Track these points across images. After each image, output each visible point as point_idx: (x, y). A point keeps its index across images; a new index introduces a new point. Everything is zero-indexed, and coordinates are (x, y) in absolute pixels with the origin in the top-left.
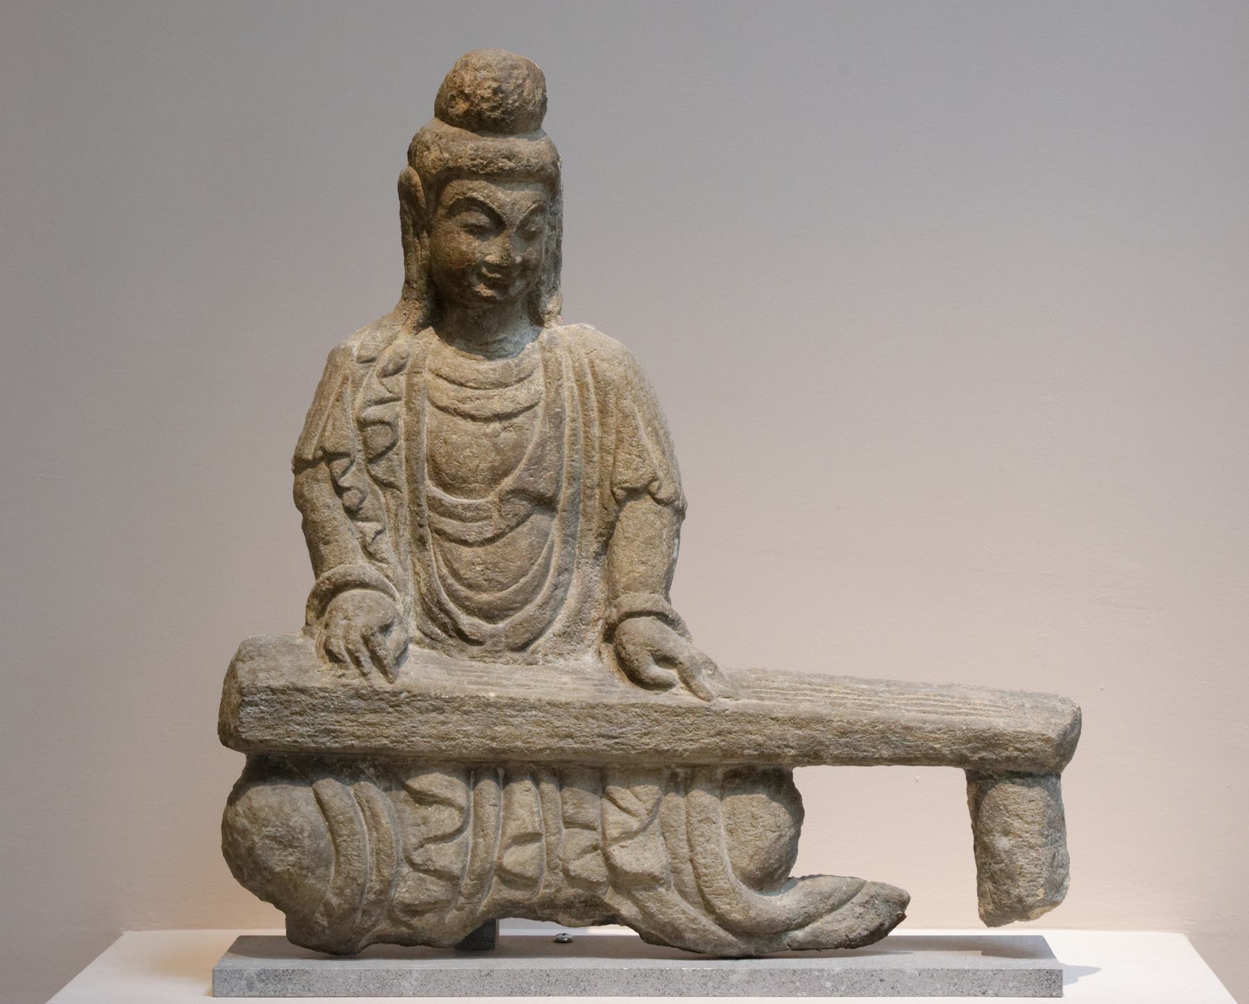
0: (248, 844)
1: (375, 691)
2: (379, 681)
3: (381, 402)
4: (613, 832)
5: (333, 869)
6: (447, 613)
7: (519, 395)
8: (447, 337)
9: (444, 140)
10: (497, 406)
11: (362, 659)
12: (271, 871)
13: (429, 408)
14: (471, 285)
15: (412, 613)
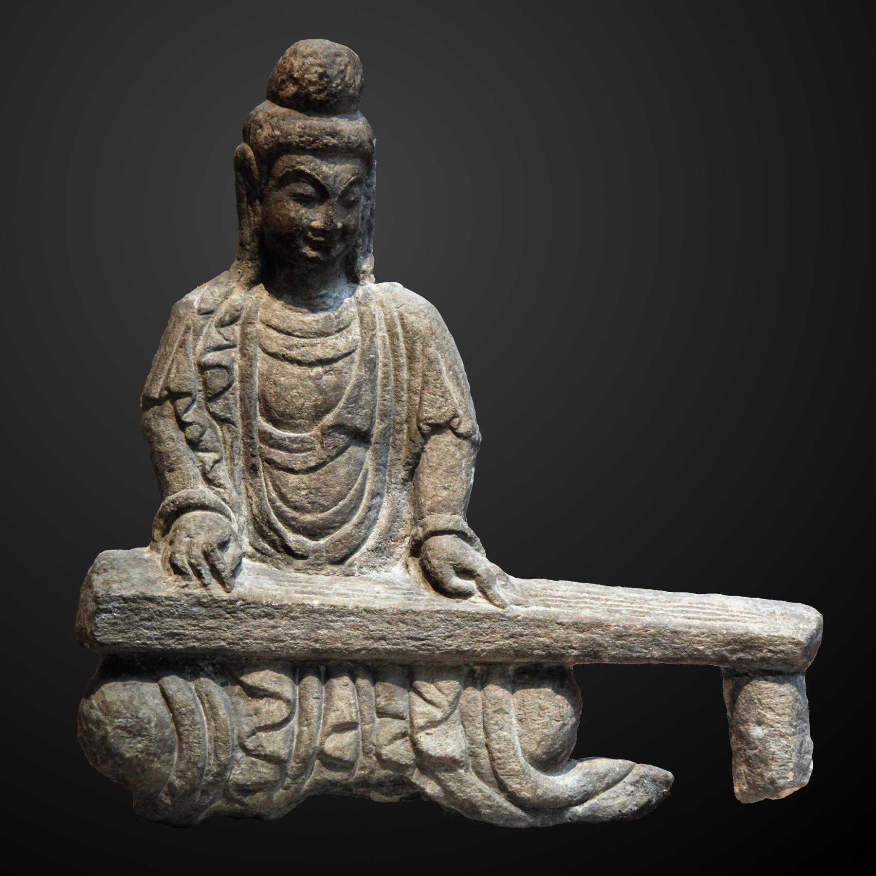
0: (101, 733)
1: (214, 599)
2: (218, 591)
3: (219, 348)
4: (420, 721)
5: (176, 755)
6: (276, 531)
7: (339, 343)
8: (276, 292)
9: (275, 119)
10: (320, 352)
11: (203, 572)
12: (122, 757)
14: (298, 248)
15: (245, 531)
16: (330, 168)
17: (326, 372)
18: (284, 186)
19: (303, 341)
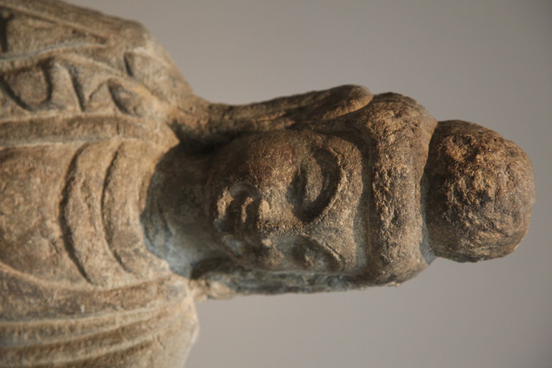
3: (77, 86)
7: (99, 258)
8: (166, 163)
9: (411, 134)
10: (82, 232)
13: (74, 146)
14: (229, 185)
16: (348, 220)
17: (53, 243)
18: (315, 156)
19: (97, 205)
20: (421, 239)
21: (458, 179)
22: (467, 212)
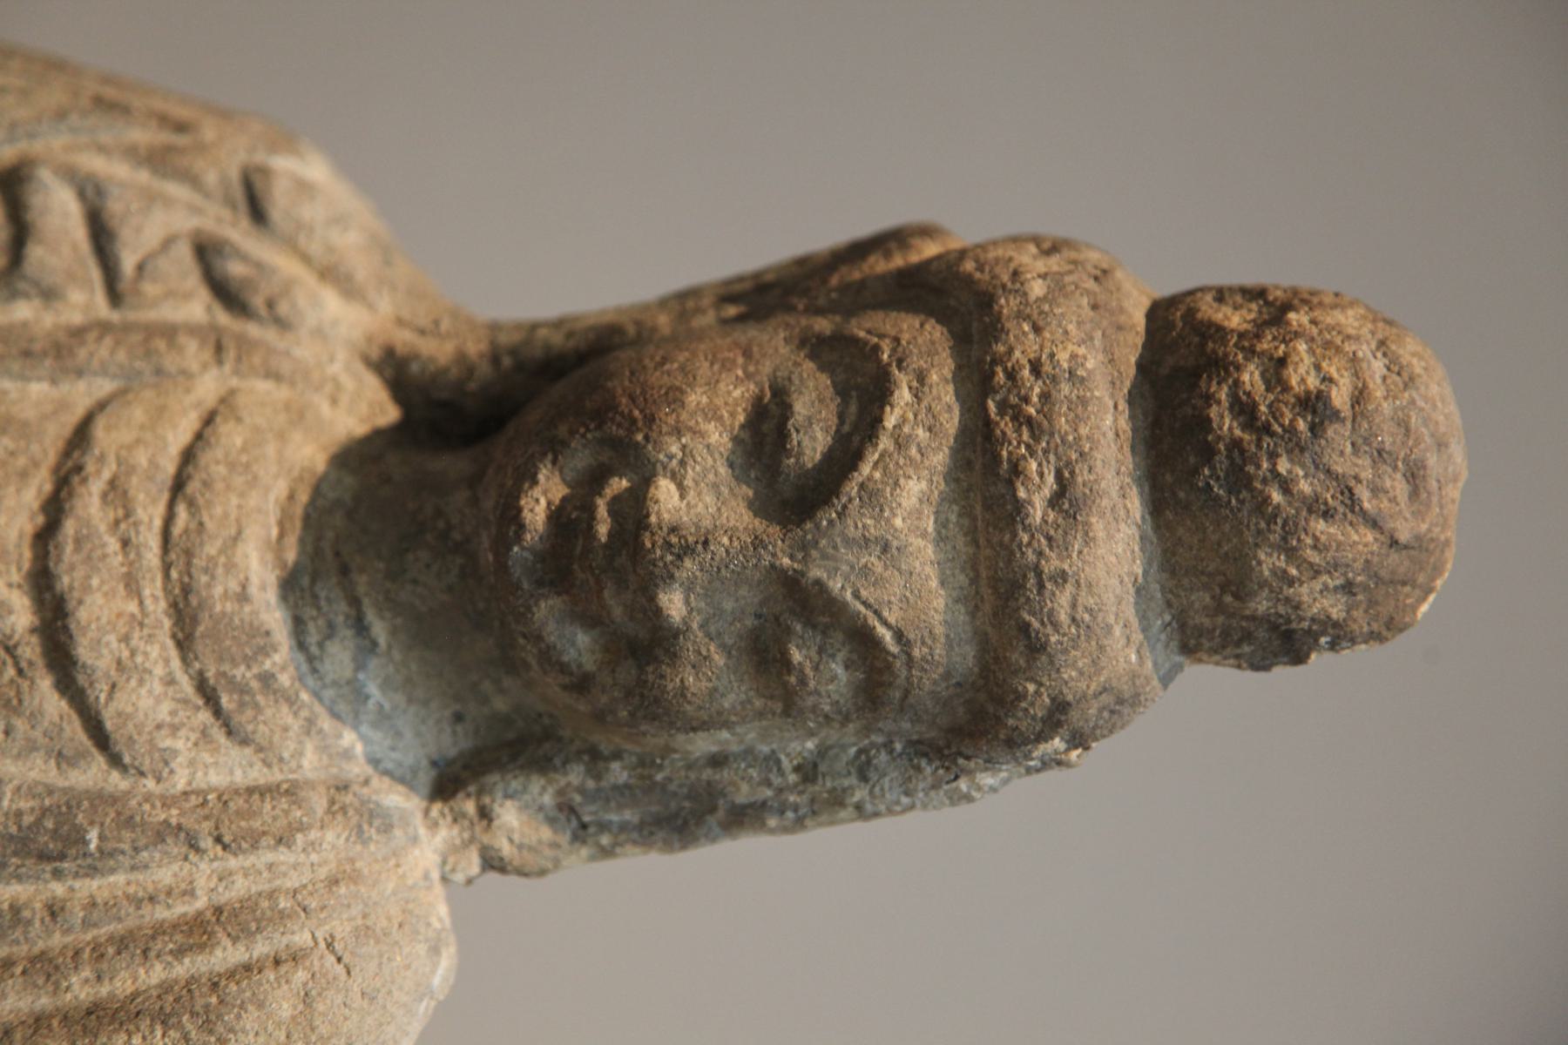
3: (101, 235)
7: (147, 689)
13: (82, 394)
14: (555, 448)
18: (812, 356)
19: (151, 541)
20: (1139, 570)
21: (1238, 368)
22: (1273, 456)
